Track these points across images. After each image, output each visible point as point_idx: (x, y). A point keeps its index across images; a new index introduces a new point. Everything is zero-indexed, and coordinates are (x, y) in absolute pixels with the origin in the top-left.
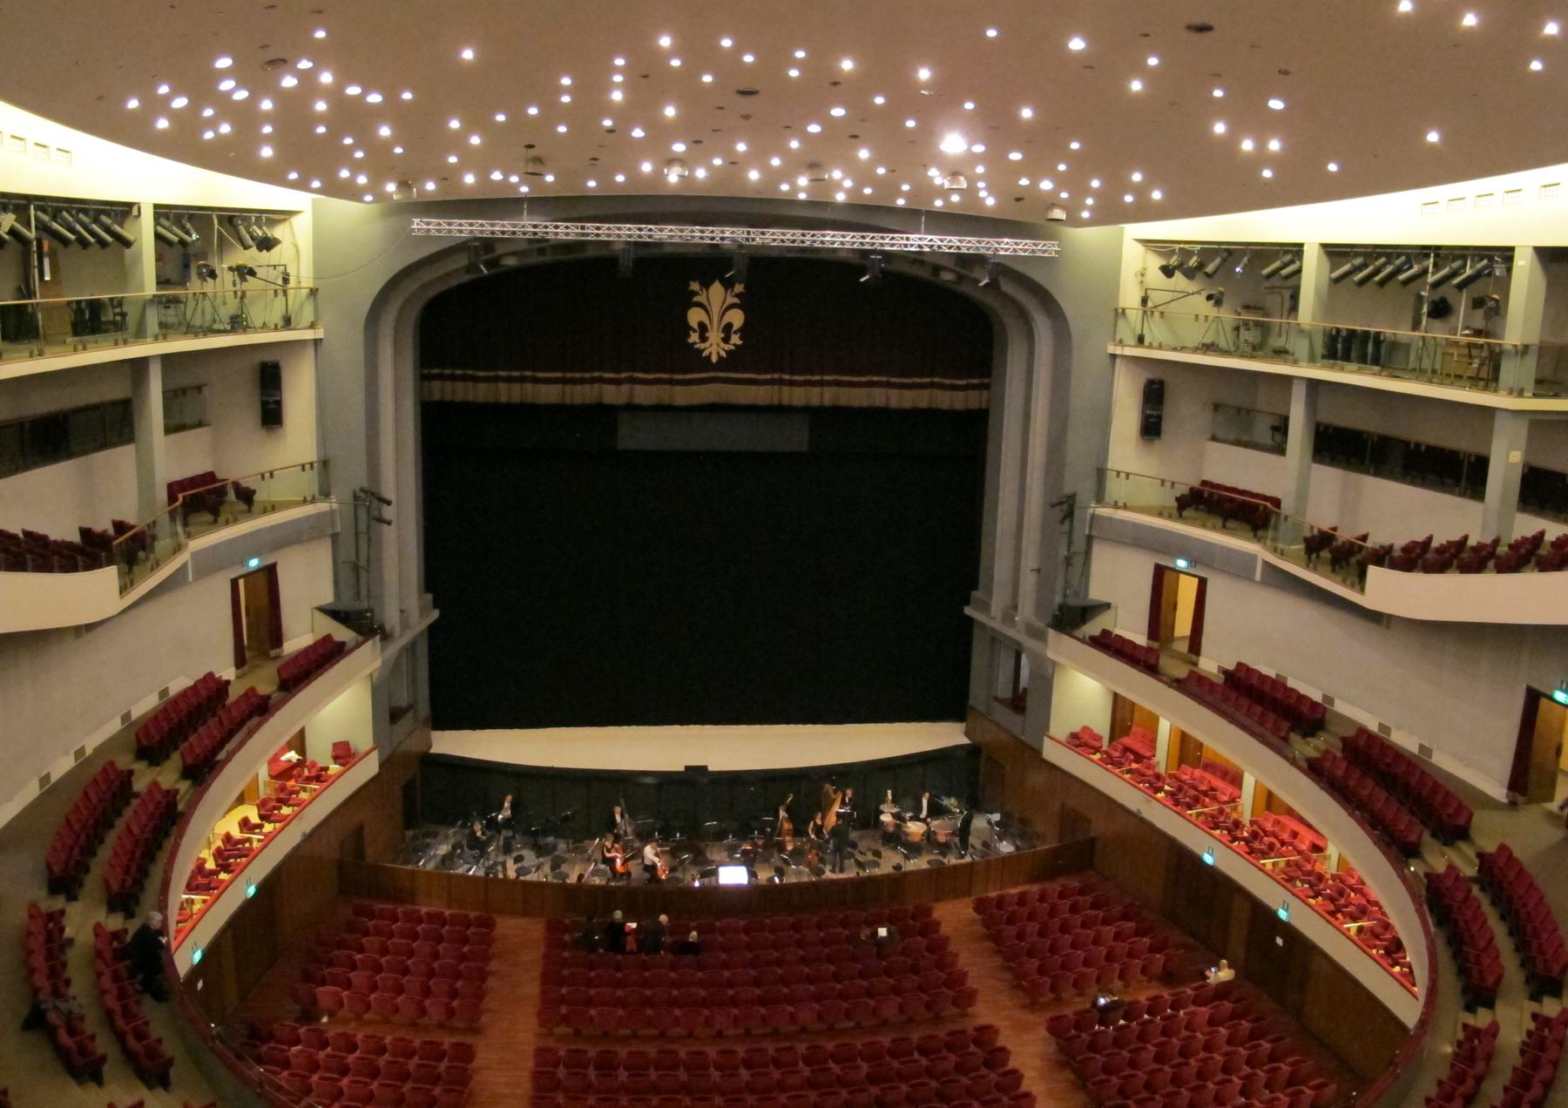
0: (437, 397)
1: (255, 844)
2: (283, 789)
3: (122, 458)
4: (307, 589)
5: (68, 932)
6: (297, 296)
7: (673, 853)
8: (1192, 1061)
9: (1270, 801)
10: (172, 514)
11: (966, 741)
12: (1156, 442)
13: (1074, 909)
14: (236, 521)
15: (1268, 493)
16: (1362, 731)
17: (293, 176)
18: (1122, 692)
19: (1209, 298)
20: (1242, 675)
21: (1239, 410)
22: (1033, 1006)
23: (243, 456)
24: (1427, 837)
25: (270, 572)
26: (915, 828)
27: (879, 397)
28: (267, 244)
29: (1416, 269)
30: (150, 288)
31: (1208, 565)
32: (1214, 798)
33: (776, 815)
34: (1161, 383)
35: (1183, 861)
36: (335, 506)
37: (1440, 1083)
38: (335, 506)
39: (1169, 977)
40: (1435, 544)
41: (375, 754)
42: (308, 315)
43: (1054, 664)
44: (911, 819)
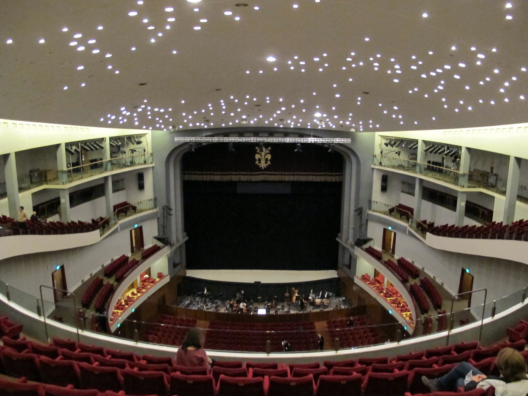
2: (143, 285)
3: (102, 199)
5: (86, 316)
6: (147, 155)
10: (114, 215)
11: (337, 276)
12: (386, 193)
14: (131, 215)
19: (396, 153)
25: (140, 228)
27: (311, 178)
28: (139, 143)
30: (109, 158)
31: (396, 229)
35: (385, 311)
40: (449, 226)
42: (150, 160)
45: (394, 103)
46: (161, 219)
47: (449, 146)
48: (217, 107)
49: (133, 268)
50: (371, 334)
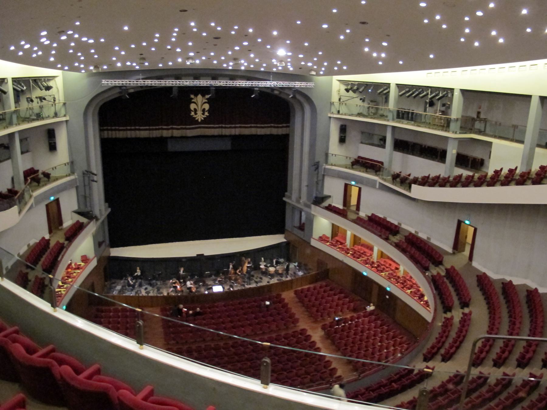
0: (106, 136)
1: (63, 293)
2: (68, 273)
4: (69, 205)
6: (59, 106)
7: (195, 283)
8: (365, 334)
9: (382, 255)
11: (285, 240)
12: (344, 145)
13: (325, 292)
14: (46, 185)
15: (379, 160)
16: (411, 234)
17: (59, 66)
18: (334, 223)
19: (361, 99)
20: (373, 217)
21: (370, 134)
22: (316, 321)
24: (431, 265)
25: (57, 201)
26: (272, 269)
28: (48, 88)
29: (425, 93)
31: (362, 183)
32: (365, 255)
33: (229, 268)
34: (345, 126)
35: (357, 274)
36: (77, 177)
37: (439, 334)
38: (77, 177)
39: (355, 310)
40: (431, 177)
42: (63, 112)
43: (314, 215)
44: (270, 266)
45: (387, 37)
46: (81, 189)
48: (165, 39)
49: (62, 253)
50: (347, 299)
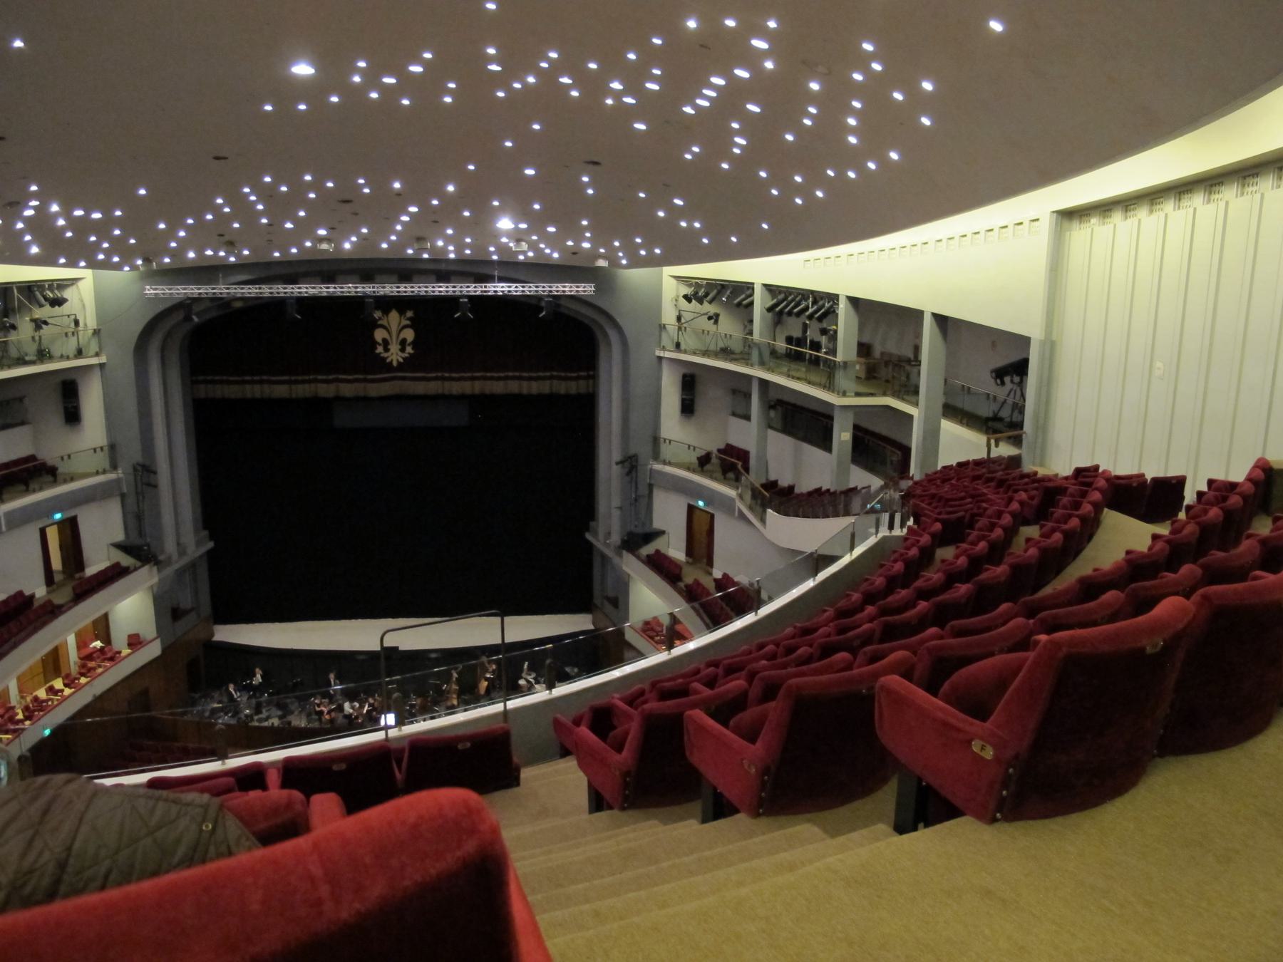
0: (202, 395)
2: (83, 666)
4: (102, 533)
11: (592, 627)
19: (710, 318)
23: (52, 442)
27: (513, 387)
41: (158, 642)
42: (94, 347)
46: (131, 500)
47: (817, 296)
